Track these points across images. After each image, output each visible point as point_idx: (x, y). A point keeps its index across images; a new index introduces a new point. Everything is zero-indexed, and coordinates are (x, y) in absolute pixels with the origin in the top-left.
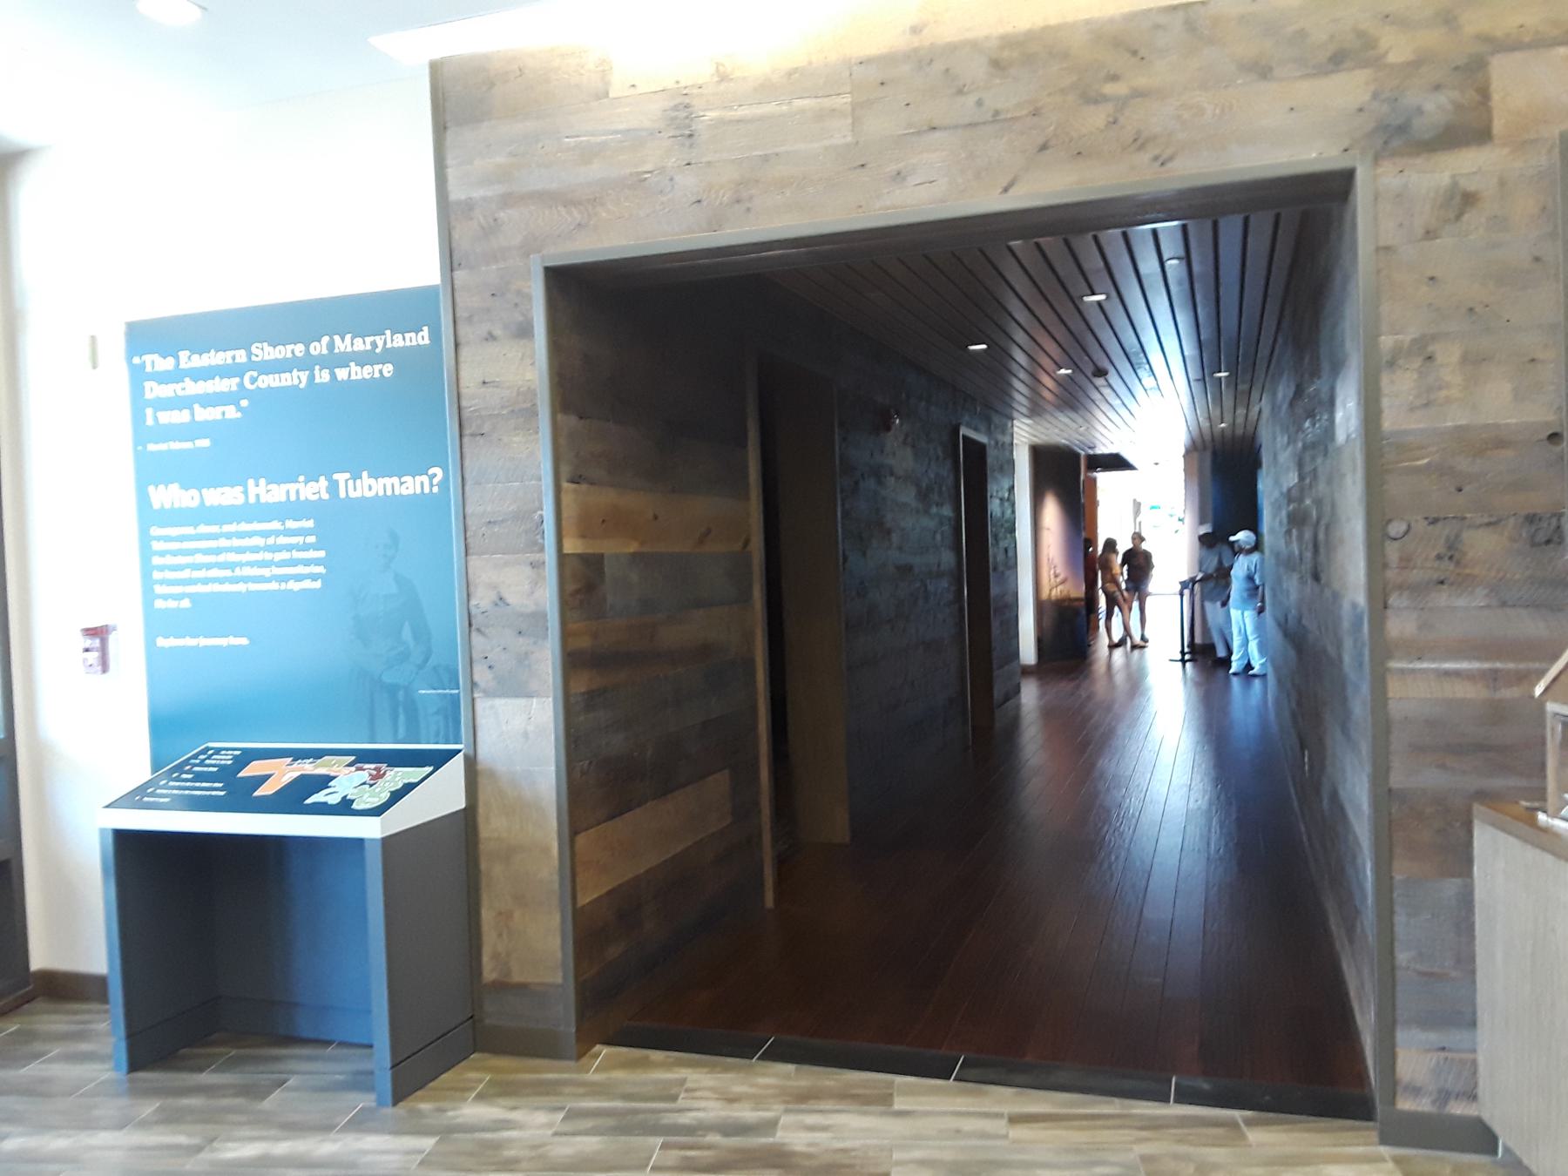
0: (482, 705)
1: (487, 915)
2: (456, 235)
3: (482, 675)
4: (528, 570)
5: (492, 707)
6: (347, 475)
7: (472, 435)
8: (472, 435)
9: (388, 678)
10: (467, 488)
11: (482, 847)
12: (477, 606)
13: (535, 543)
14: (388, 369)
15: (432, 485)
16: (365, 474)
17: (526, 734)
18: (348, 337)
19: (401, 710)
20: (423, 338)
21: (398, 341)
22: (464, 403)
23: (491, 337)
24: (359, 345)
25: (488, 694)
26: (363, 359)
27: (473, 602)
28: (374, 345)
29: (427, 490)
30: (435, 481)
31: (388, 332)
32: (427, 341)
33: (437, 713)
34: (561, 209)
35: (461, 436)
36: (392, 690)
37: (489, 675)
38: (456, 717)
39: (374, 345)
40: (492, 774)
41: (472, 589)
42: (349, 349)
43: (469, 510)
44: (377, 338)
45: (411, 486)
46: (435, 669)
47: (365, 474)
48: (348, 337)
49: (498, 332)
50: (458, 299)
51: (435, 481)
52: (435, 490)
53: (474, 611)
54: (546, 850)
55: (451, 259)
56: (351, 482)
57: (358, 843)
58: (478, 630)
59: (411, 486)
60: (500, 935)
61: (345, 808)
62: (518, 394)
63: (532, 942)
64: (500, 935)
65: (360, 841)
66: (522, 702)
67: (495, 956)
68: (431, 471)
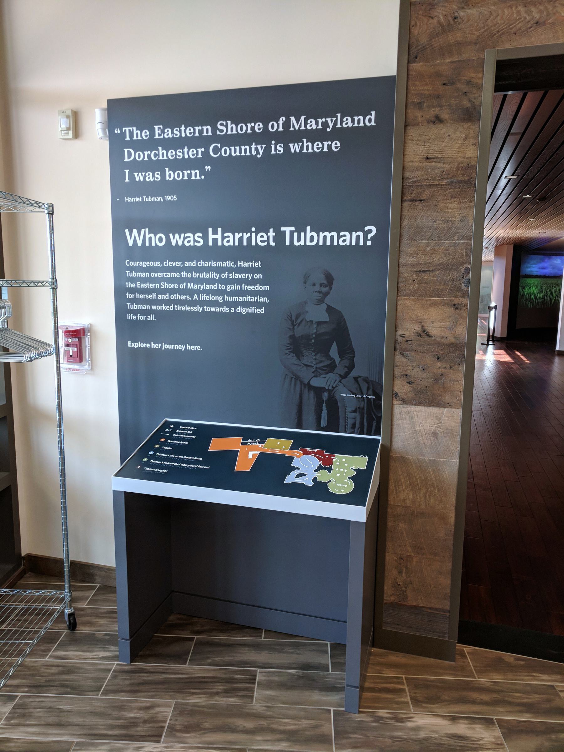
0: (399, 409)
1: (390, 558)
2: (415, 31)
3: (400, 387)
4: (450, 311)
5: (407, 412)
6: (293, 229)
7: (413, 200)
8: (413, 200)
9: (316, 382)
10: (404, 242)
11: (389, 510)
12: (402, 336)
13: (459, 289)
14: (336, 145)
15: (366, 239)
16: (308, 228)
17: (435, 434)
18: (303, 118)
19: (324, 408)
20: (370, 120)
21: (348, 123)
22: (407, 174)
23: (438, 120)
24: (312, 125)
25: (405, 402)
26: (313, 136)
27: (400, 332)
28: (325, 125)
29: (361, 243)
30: (370, 236)
31: (339, 115)
32: (373, 123)
33: (355, 411)
34: (521, 9)
35: (402, 201)
36: (318, 391)
37: (408, 388)
38: (372, 416)
39: (325, 125)
40: (404, 460)
41: (399, 323)
42: (303, 128)
43: (403, 260)
44: (329, 120)
45: (347, 239)
46: (356, 379)
47: (308, 228)
48: (303, 118)
49: (445, 115)
50: (411, 88)
51: (370, 236)
52: (369, 243)
53: (399, 339)
54: (443, 518)
55: (409, 48)
56: (295, 234)
57: (345, 524)
58: (402, 354)
59: (347, 239)
60: (400, 572)
61: (319, 492)
62: (458, 168)
63: (432, 579)
64: (400, 572)
65: (346, 523)
66: (435, 410)
67: (396, 585)
68: (366, 229)
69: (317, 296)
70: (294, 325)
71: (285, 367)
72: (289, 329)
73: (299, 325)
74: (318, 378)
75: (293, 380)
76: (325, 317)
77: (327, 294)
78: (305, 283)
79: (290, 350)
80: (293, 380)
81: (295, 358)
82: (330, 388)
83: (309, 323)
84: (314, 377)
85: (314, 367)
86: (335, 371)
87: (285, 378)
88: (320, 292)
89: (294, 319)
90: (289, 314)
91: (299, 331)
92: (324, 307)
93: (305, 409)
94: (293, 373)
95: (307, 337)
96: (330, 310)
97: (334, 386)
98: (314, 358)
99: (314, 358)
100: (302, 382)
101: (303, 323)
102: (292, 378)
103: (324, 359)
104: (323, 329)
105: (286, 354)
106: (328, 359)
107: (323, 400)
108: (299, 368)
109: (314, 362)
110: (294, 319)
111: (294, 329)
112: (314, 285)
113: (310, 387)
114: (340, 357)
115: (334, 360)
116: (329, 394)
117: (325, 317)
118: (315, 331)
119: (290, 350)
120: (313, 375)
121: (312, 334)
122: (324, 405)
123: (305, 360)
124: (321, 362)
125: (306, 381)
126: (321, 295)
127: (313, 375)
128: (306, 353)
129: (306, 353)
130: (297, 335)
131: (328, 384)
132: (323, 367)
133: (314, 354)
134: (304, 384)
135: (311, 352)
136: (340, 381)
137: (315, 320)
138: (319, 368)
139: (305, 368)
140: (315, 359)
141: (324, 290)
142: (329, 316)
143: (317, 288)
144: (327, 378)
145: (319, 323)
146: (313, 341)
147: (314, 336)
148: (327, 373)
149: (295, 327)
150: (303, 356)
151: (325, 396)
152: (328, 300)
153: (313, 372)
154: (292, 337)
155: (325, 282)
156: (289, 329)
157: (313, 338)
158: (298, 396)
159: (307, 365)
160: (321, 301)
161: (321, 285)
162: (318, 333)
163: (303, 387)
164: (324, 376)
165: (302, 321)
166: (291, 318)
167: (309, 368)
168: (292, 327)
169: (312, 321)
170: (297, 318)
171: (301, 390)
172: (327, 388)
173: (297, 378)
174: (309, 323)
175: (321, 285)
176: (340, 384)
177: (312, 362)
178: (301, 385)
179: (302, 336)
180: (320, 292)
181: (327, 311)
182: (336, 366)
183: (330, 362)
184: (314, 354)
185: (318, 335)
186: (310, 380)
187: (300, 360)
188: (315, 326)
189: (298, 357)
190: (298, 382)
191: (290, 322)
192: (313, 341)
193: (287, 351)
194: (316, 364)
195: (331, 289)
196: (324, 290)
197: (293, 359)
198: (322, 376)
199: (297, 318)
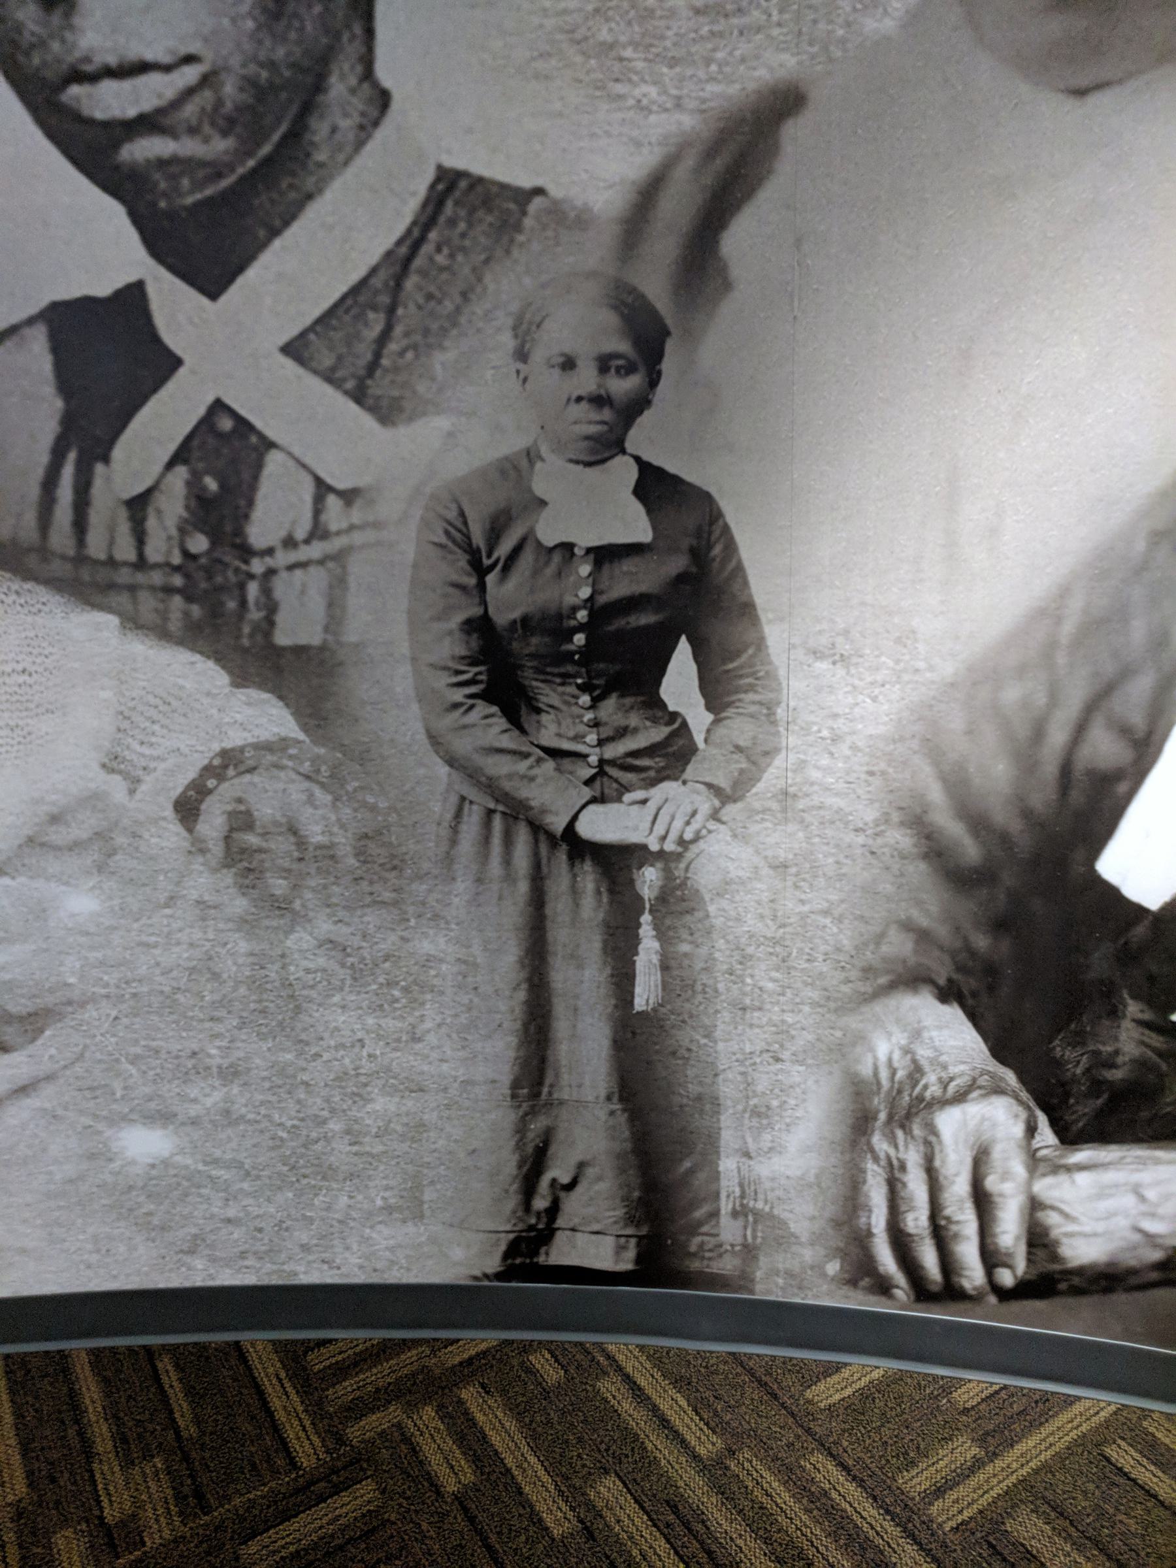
69: (588, 422)
70: (481, 571)
71: (452, 762)
72: (463, 588)
73: (506, 569)
74: (614, 807)
75: (497, 822)
76: (636, 526)
77: (634, 409)
78: (522, 355)
79: (473, 689)
80: (497, 823)
81: (501, 723)
82: (670, 846)
83: (557, 558)
84: (593, 800)
85: (593, 760)
86: (690, 772)
87: (458, 815)
88: (599, 401)
89: (478, 539)
90: (452, 515)
91: (509, 598)
92: (624, 472)
93: (560, 935)
94: (490, 786)
95: (554, 625)
96: (655, 486)
97: (688, 836)
98: (589, 716)
99: (589, 716)
100: (537, 828)
101: (527, 558)
102: (490, 812)
103: (634, 720)
104: (622, 583)
105: (456, 706)
106: (655, 720)
107: (640, 899)
108: (522, 766)
109: (592, 738)
110: (478, 539)
111: (482, 586)
112: (569, 364)
113: (577, 847)
114: (709, 708)
115: (684, 724)
116: (668, 875)
117: (636, 526)
118: (585, 592)
119: (473, 689)
120: (587, 793)
121: (574, 609)
122: (646, 918)
123: (549, 732)
124: (622, 732)
125: (558, 824)
126: (607, 414)
127: (587, 793)
128: (548, 695)
129: (548, 695)
130: (502, 617)
131: (660, 829)
132: (635, 754)
133: (585, 699)
134: (550, 836)
135: (572, 689)
136: (715, 816)
137: (586, 538)
138: (612, 763)
139: (550, 765)
140: (596, 724)
141: (622, 386)
142: (649, 512)
143: (587, 380)
144: (652, 806)
145: (604, 555)
146: (579, 639)
147: (582, 615)
148: (653, 783)
149: (491, 579)
150: (538, 711)
151: (649, 879)
152: (645, 439)
153: (588, 782)
154: (480, 627)
155: (623, 346)
156: (463, 588)
157: (580, 628)
158: (523, 887)
159: (554, 753)
160: (606, 446)
161: (604, 364)
162: (602, 600)
163: (544, 849)
164: (639, 795)
165: (517, 550)
166: (468, 537)
167: (567, 763)
168: (472, 581)
169: (567, 548)
170: (495, 533)
171: (537, 866)
172: (654, 847)
173: (516, 812)
174: (557, 558)
175: (604, 364)
176: (712, 825)
177: (578, 738)
178: (536, 841)
179: (525, 620)
180: (599, 401)
181: (640, 492)
182: (692, 749)
183: (665, 731)
184: (585, 699)
185: (602, 613)
186: (575, 818)
187: (523, 731)
188: (585, 569)
189: (515, 722)
190: (523, 836)
191: (463, 560)
192: (579, 639)
193: (458, 695)
194: (601, 743)
195: (653, 381)
196: (622, 386)
197: (487, 728)
198: (628, 797)
199: (495, 533)
